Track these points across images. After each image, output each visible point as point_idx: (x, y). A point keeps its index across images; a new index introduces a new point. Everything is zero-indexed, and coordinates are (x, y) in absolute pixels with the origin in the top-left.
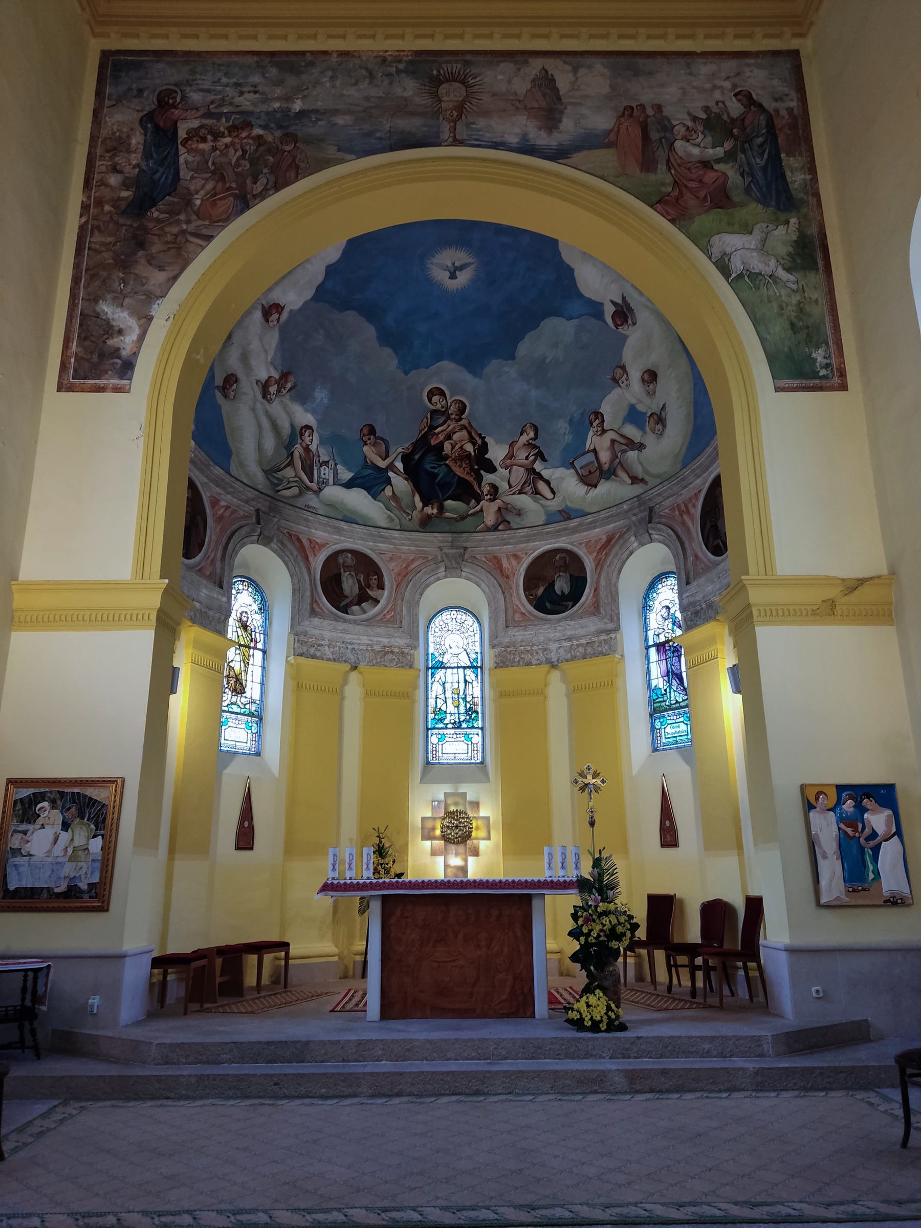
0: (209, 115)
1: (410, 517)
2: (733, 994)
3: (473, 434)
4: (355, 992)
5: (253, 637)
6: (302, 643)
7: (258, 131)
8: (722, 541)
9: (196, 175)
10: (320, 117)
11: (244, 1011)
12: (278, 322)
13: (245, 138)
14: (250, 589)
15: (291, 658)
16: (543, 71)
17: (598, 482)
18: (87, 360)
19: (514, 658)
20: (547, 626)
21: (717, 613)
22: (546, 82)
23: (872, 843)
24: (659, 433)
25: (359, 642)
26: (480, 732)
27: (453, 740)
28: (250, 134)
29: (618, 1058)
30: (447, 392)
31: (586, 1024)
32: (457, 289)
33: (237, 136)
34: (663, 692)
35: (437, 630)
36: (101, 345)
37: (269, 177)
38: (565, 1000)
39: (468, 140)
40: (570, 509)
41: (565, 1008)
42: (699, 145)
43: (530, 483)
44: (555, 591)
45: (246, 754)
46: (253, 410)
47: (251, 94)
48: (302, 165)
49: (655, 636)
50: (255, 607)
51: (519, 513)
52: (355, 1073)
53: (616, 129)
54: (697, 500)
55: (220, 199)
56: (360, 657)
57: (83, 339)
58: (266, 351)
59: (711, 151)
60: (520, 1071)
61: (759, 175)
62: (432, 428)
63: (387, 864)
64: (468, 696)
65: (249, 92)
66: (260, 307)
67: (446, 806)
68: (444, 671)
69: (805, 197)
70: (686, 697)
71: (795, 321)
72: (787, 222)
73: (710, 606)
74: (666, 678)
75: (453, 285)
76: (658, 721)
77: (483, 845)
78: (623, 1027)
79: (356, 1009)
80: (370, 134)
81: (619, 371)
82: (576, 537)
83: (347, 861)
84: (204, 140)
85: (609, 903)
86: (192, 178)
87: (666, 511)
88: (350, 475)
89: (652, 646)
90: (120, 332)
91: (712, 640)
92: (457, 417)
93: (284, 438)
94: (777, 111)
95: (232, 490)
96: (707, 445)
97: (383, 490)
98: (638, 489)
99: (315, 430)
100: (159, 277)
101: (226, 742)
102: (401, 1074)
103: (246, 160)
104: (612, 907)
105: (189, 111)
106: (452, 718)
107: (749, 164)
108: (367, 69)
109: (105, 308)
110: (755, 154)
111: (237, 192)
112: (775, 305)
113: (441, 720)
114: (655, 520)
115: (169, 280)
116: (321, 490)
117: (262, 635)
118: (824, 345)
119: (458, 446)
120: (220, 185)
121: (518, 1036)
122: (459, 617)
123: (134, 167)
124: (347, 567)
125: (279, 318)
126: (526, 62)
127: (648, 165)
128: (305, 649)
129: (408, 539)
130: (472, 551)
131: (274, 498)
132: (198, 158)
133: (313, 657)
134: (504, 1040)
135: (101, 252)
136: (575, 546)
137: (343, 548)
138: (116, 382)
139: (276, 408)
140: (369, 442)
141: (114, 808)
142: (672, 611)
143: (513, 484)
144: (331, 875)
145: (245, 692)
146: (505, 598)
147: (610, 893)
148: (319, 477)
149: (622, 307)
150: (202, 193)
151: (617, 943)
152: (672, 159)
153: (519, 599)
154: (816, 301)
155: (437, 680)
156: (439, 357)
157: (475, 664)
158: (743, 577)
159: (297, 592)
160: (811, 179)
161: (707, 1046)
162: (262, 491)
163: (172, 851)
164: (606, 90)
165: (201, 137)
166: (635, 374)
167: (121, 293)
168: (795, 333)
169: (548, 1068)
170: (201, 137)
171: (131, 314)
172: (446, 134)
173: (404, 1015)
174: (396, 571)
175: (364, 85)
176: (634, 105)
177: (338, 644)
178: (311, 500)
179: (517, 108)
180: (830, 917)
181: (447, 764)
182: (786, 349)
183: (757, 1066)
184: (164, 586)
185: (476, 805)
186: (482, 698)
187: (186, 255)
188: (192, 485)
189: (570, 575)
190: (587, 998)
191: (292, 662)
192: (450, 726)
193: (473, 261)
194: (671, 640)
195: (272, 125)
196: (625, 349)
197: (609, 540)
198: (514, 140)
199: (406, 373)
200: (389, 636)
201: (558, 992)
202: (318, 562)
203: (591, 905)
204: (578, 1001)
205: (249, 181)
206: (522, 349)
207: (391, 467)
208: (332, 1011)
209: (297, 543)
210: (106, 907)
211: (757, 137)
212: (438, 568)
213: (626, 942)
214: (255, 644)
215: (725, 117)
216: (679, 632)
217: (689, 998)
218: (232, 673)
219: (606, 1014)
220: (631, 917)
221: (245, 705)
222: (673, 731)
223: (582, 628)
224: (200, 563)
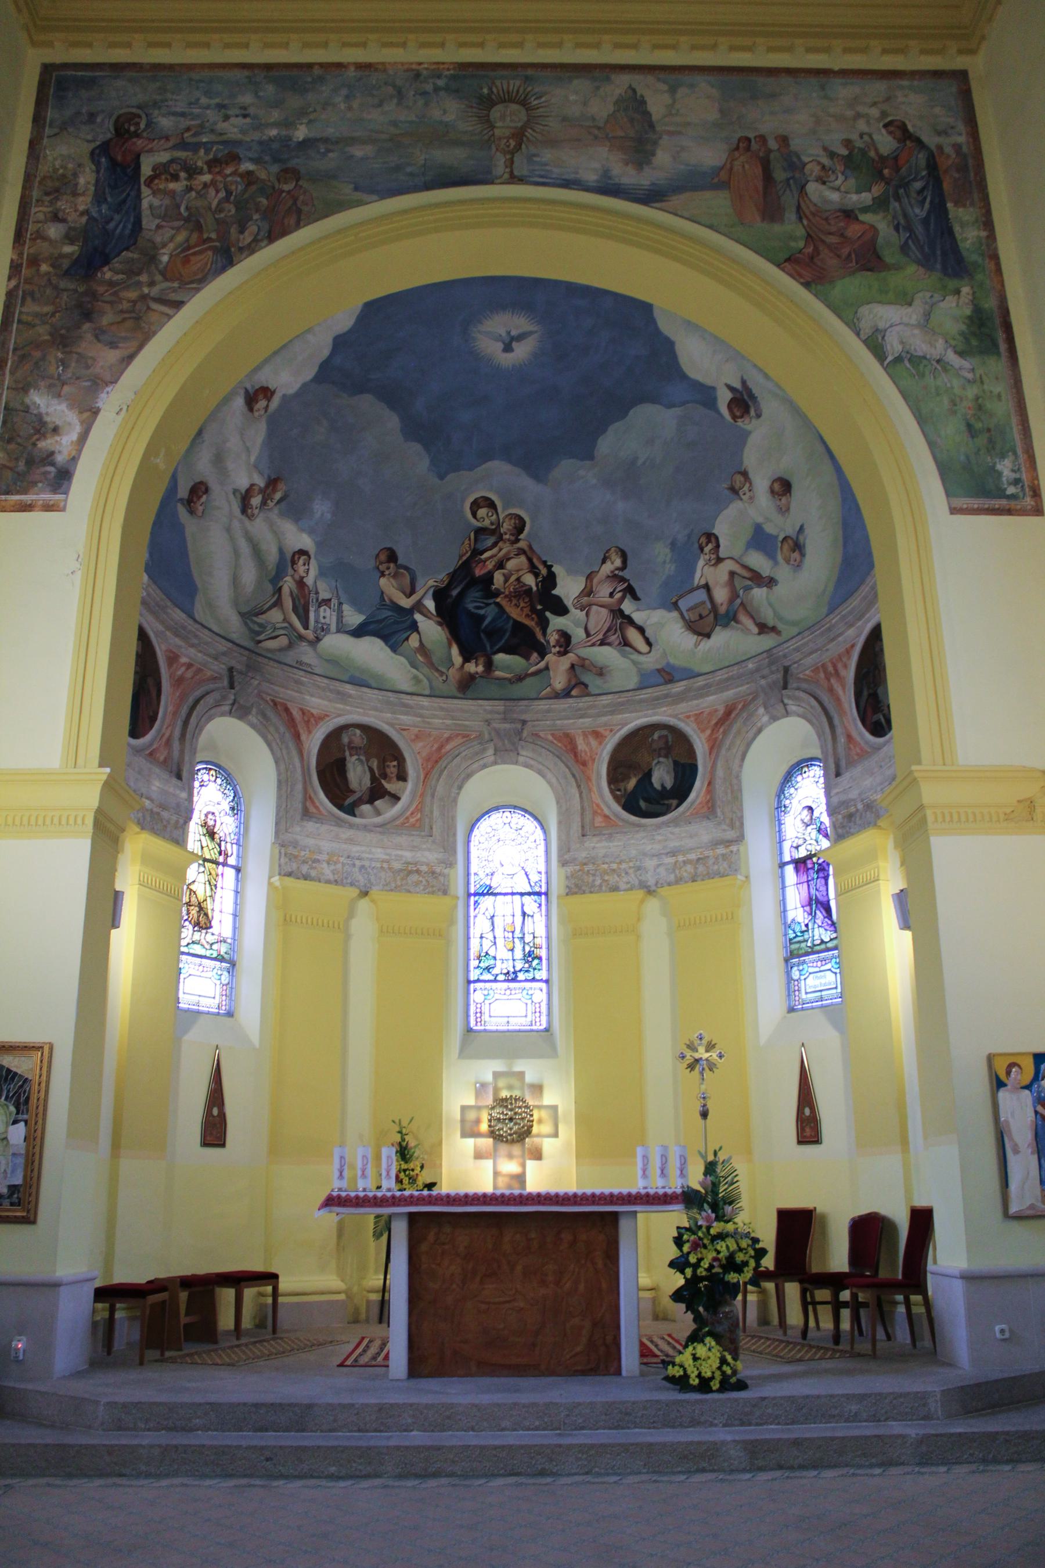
0: (183, 145)
1: (444, 678)
2: (889, 1337)
3: (535, 561)
4: (370, 1341)
5: (223, 848)
6: (292, 857)
7: (247, 166)
8: (884, 715)
9: (164, 223)
11: (220, 1362)
12: (266, 411)
13: (230, 175)
14: (219, 781)
15: (276, 879)
16: (630, 92)
17: (712, 630)
18: (11, 469)
19: (594, 881)
20: (642, 834)
21: (878, 817)
24: (796, 564)
25: (370, 856)
26: (543, 985)
27: (505, 997)
28: (236, 170)
29: (734, 1425)
30: (499, 505)
31: (691, 1382)
32: (513, 366)
33: (219, 173)
34: (804, 928)
35: (482, 840)
36: (30, 448)
37: (260, 224)
38: (661, 1351)
39: (529, 176)
40: (673, 667)
41: (663, 1362)
42: (838, 189)
43: (616, 630)
44: (651, 784)
45: (213, 1014)
46: (228, 530)
47: (240, 119)
48: (305, 209)
49: (793, 850)
50: (226, 805)
51: (601, 672)
52: (375, 1447)
53: (728, 166)
54: (849, 658)
55: (195, 254)
56: (372, 878)
58: (248, 450)
59: (854, 197)
60: (601, 1445)
61: (919, 230)
62: (476, 552)
63: (413, 1170)
64: (526, 935)
65: (237, 116)
66: (242, 392)
67: (496, 1090)
68: (492, 898)
69: (980, 260)
70: (834, 935)
71: (972, 421)
72: (957, 292)
73: (869, 807)
74: (807, 909)
75: (507, 360)
76: (795, 968)
77: (548, 1146)
78: (741, 1386)
79: (374, 1363)
80: (398, 168)
81: (739, 478)
82: (682, 707)
83: (359, 1165)
84: (175, 178)
85: (727, 1222)
86: (159, 227)
87: (807, 672)
89: (788, 863)
90: (56, 430)
91: (871, 856)
92: (513, 538)
93: (270, 568)
95: (196, 641)
96: (862, 582)
97: (407, 639)
98: (767, 641)
99: (312, 556)
101: (186, 996)
102: (438, 1448)
103: (230, 203)
104: (730, 1227)
105: (156, 142)
106: (504, 966)
107: (905, 215)
108: (394, 86)
109: (37, 400)
110: (913, 201)
112: (946, 401)
113: (488, 969)
114: (793, 684)
115: (123, 360)
116: (318, 639)
117: (234, 846)
118: (1010, 454)
119: (513, 578)
120: (195, 236)
121: (599, 1399)
122: (514, 821)
123: (82, 214)
124: (354, 749)
125: (267, 406)
126: (608, 79)
127: (771, 212)
128: (294, 866)
129: (442, 709)
130: (534, 726)
131: (253, 652)
132: (167, 201)
133: (306, 877)
134: (579, 1404)
135: (34, 326)
136: (679, 719)
137: (349, 722)
138: (48, 497)
139: (259, 526)
140: (387, 572)
141: (39, 1084)
142: (816, 814)
143: (592, 633)
144: (337, 1184)
145: (211, 927)
146: (581, 794)
147: (728, 1209)
148: (317, 622)
149: (741, 393)
150: (171, 246)
151: (736, 1275)
152: (803, 205)
154: (999, 396)
155: (482, 911)
156: (486, 456)
157: (537, 889)
158: (914, 768)
159: (283, 784)
160: (988, 237)
161: (854, 1408)
162: (238, 641)
163: (116, 1146)
164: (713, 115)
165: (172, 175)
166: (761, 484)
167: (59, 379)
168: (973, 437)
169: (640, 1439)
170: (172, 175)
171: (71, 407)
172: (500, 167)
173: (438, 1372)
174: (424, 754)
175: (391, 106)
176: (751, 135)
177: (342, 859)
178: (305, 653)
181: (497, 1031)
182: (962, 458)
184: (104, 777)
185: (538, 1089)
186: (548, 938)
187: (147, 327)
188: (143, 635)
189: (676, 763)
190: (694, 1348)
191: (277, 884)
192: (501, 977)
193: (535, 329)
194: (815, 855)
196: (747, 450)
197: (728, 713)
198: (591, 177)
199: (441, 477)
200: (413, 848)
201: (652, 1342)
202: (314, 741)
203: (700, 1227)
204: (680, 1353)
205: (234, 230)
206: (605, 445)
207: (419, 606)
208: (341, 1365)
209: (284, 715)
210: (32, 1218)
212: (484, 750)
213: (748, 1274)
214: (226, 859)
215: (872, 154)
216: (825, 843)
217: (831, 1345)
218: (193, 899)
219: (719, 1368)
220: (756, 1241)
221: (212, 945)
222: (817, 982)
223: (691, 837)
224: (151, 744)
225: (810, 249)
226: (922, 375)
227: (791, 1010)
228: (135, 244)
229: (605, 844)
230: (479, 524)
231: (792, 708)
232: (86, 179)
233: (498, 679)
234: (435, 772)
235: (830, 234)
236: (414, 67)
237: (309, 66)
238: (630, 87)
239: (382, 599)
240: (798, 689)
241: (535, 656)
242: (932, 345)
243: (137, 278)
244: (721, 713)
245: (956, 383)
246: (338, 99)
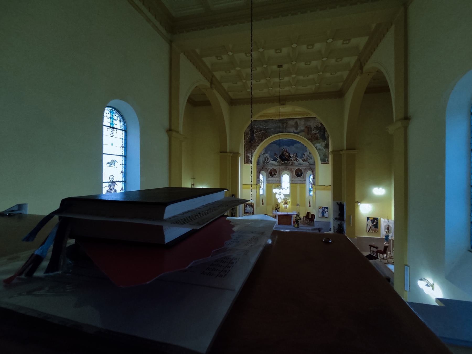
0: (257, 129)
7: (263, 131)
22: (296, 123)
51: (294, 163)
57: (246, 158)
59: (316, 132)
62: (283, 153)
72: (325, 142)
77: (289, 204)
78: (299, 227)
82: (302, 168)
84: (257, 133)
98: (309, 164)
116: (269, 162)
124: (272, 171)
127: (308, 134)
166: (308, 152)
176: (307, 125)
185: (288, 199)
197: (306, 169)
198: (292, 131)
206: (295, 145)
207: (278, 158)
215: (318, 127)
227: (310, 195)
232: (249, 133)
237: (267, 120)
238: (296, 121)
244: (305, 168)
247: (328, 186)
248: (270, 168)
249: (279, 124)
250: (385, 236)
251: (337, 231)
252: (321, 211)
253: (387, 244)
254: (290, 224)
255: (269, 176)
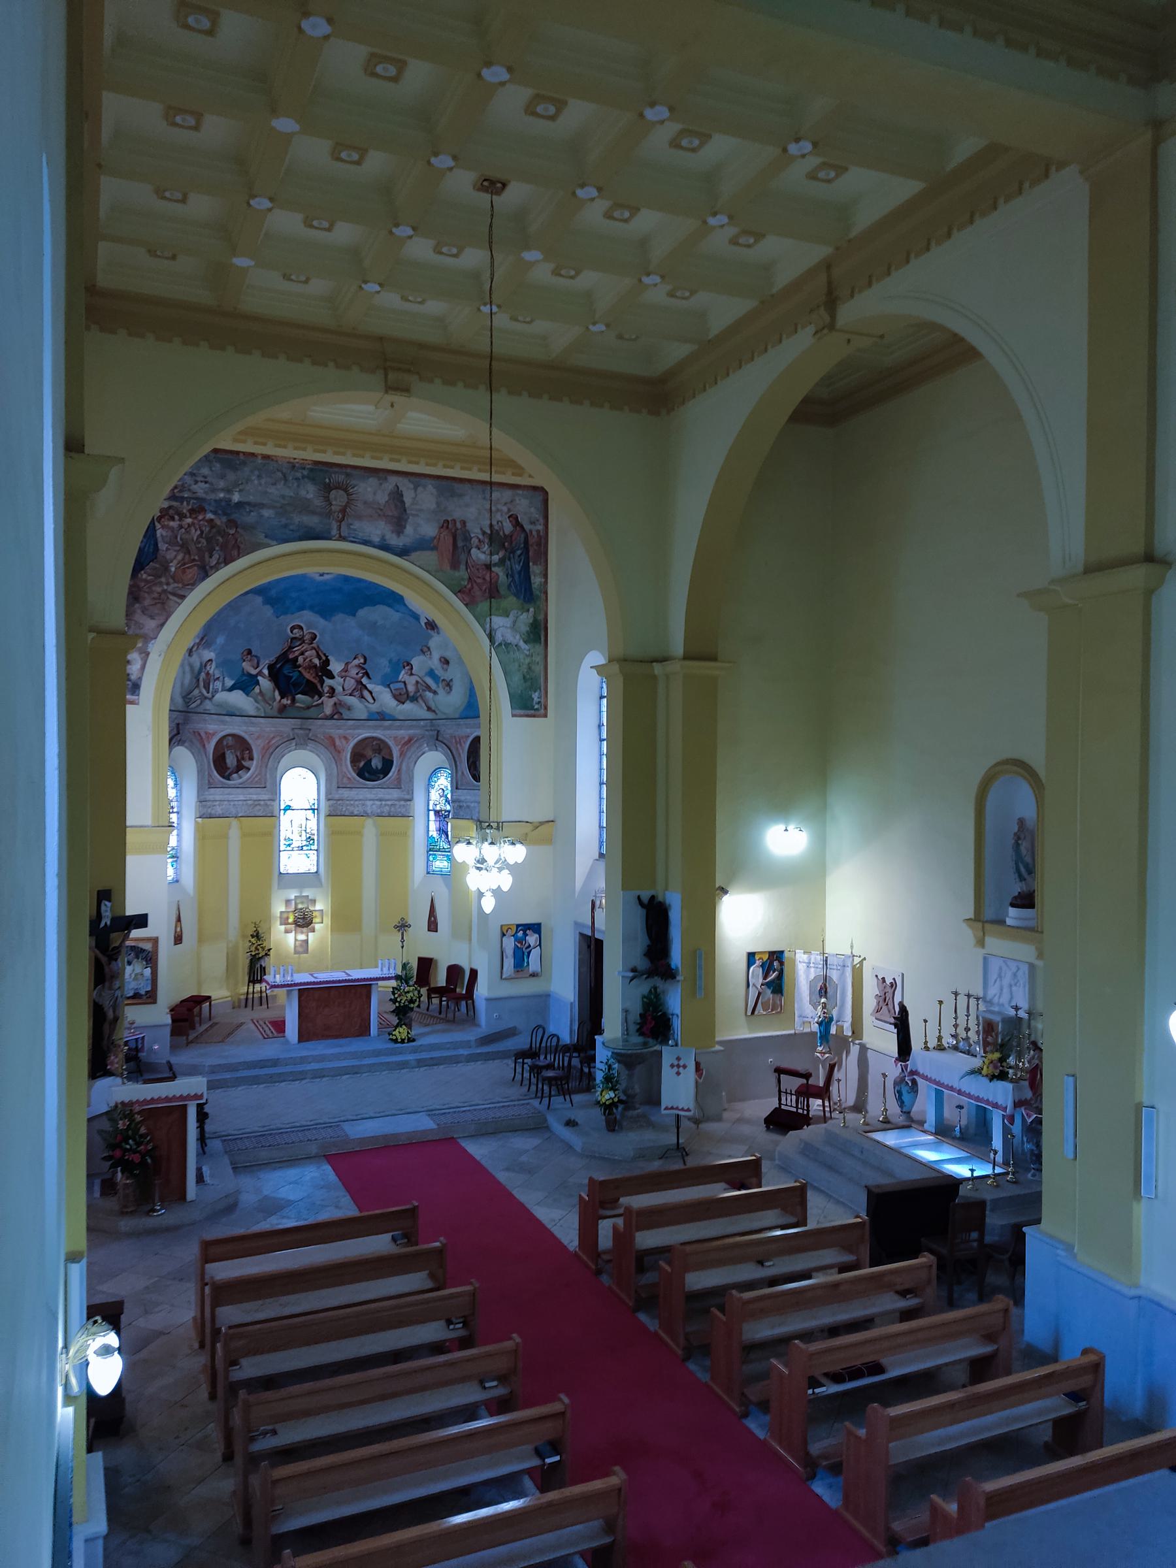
6: (204, 806)
7: (210, 516)
10: (252, 509)
22: (397, 496)
23: (528, 950)
26: (315, 852)
33: (196, 518)
42: (484, 553)
48: (242, 546)
51: (349, 708)
55: (188, 568)
61: (517, 577)
62: (291, 648)
65: (201, 482)
72: (528, 611)
77: (317, 926)
78: (414, 1040)
80: (286, 526)
82: (388, 732)
84: (173, 519)
86: (167, 549)
88: (232, 683)
94: (531, 531)
98: (430, 715)
100: (151, 624)
108: (282, 473)
111: (199, 563)
112: (516, 664)
116: (213, 696)
120: (187, 556)
124: (229, 747)
127: (455, 566)
142: (445, 793)
150: (175, 562)
153: (347, 768)
154: (538, 663)
156: (302, 609)
159: (200, 772)
164: (434, 506)
166: (436, 656)
174: (262, 745)
175: (280, 485)
176: (449, 519)
178: (208, 705)
179: (379, 515)
180: (505, 983)
183: (469, 1053)
185: (314, 902)
186: (318, 830)
189: (383, 758)
195: (220, 512)
197: (410, 740)
198: (376, 540)
199: (277, 617)
202: (211, 747)
205: (207, 555)
206: (362, 613)
207: (260, 673)
211: (518, 549)
215: (501, 533)
225: (470, 585)
226: (508, 652)
227: (428, 873)
228: (156, 558)
229: (348, 792)
230: (294, 636)
231: (439, 749)
233: (298, 707)
234: (267, 755)
235: (479, 577)
236: (292, 460)
237: (238, 453)
239: (243, 671)
240: (442, 742)
241: (316, 697)
242: (515, 638)
243: (158, 581)
244: (406, 739)
245: (522, 656)
246: (253, 478)
247: (542, 823)
248: (217, 729)
249: (310, 492)
250: (820, 1024)
251: (638, 1030)
252: (509, 944)
253: (827, 1055)
254: (364, 1031)
255: (210, 776)
